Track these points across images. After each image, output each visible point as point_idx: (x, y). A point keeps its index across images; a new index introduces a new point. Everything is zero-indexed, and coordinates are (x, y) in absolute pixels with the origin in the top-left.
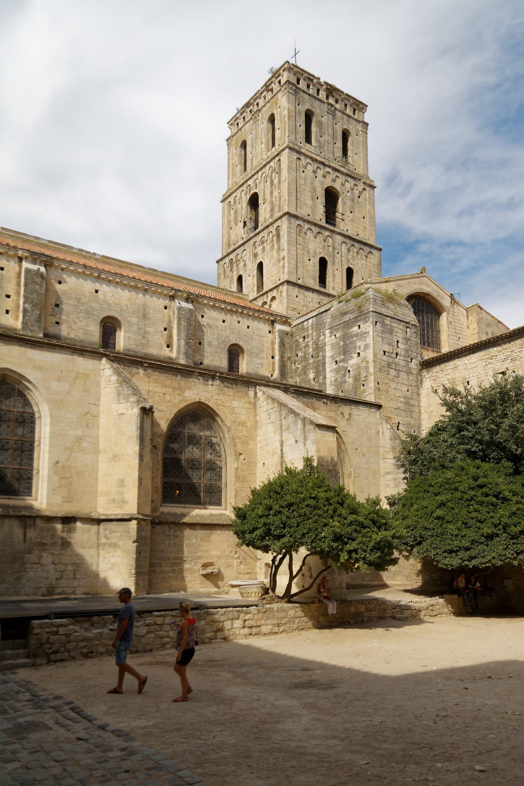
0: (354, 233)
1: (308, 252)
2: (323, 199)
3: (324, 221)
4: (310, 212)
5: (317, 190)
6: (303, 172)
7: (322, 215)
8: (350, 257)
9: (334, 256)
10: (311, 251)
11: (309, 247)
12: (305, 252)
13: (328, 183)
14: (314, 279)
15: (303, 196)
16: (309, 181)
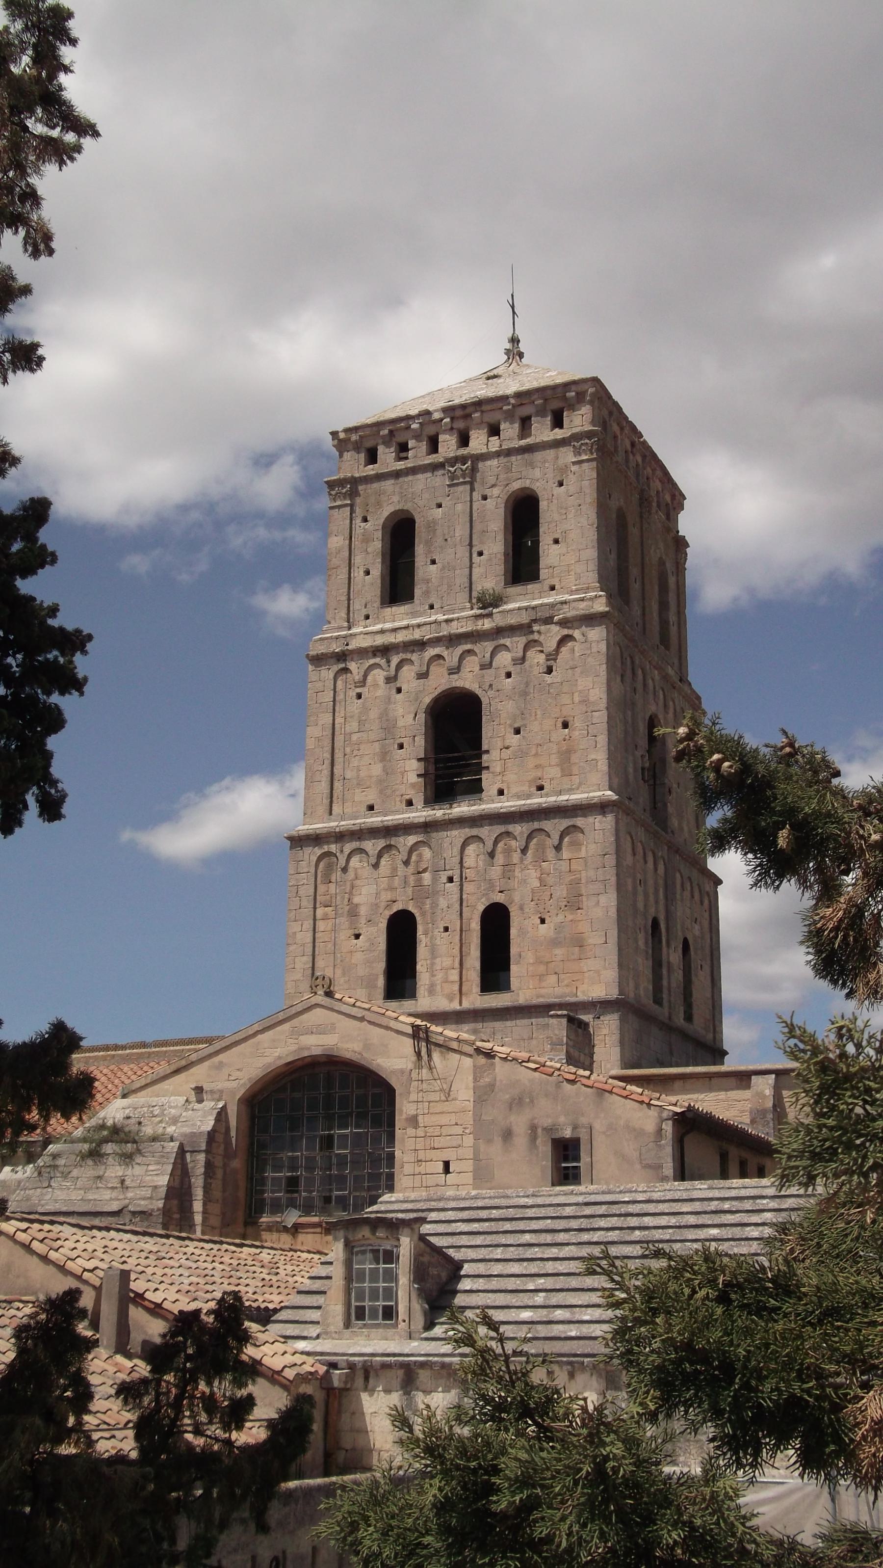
0: (525, 788)
1: (353, 913)
2: (420, 741)
3: (419, 800)
4: (371, 797)
5: (401, 723)
6: (359, 696)
7: (413, 785)
8: (496, 872)
9: (433, 893)
10: (363, 911)
11: (356, 900)
12: (343, 921)
13: (440, 681)
14: (371, 985)
15: (355, 762)
16: (374, 714)
